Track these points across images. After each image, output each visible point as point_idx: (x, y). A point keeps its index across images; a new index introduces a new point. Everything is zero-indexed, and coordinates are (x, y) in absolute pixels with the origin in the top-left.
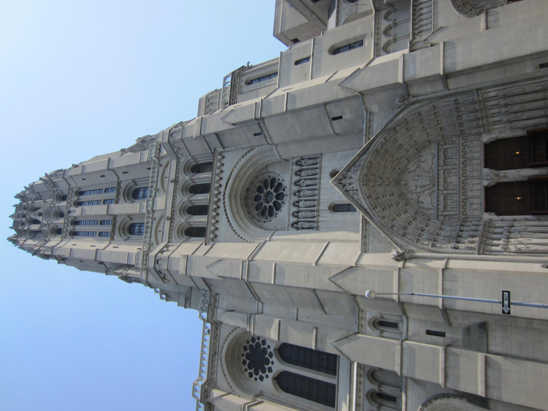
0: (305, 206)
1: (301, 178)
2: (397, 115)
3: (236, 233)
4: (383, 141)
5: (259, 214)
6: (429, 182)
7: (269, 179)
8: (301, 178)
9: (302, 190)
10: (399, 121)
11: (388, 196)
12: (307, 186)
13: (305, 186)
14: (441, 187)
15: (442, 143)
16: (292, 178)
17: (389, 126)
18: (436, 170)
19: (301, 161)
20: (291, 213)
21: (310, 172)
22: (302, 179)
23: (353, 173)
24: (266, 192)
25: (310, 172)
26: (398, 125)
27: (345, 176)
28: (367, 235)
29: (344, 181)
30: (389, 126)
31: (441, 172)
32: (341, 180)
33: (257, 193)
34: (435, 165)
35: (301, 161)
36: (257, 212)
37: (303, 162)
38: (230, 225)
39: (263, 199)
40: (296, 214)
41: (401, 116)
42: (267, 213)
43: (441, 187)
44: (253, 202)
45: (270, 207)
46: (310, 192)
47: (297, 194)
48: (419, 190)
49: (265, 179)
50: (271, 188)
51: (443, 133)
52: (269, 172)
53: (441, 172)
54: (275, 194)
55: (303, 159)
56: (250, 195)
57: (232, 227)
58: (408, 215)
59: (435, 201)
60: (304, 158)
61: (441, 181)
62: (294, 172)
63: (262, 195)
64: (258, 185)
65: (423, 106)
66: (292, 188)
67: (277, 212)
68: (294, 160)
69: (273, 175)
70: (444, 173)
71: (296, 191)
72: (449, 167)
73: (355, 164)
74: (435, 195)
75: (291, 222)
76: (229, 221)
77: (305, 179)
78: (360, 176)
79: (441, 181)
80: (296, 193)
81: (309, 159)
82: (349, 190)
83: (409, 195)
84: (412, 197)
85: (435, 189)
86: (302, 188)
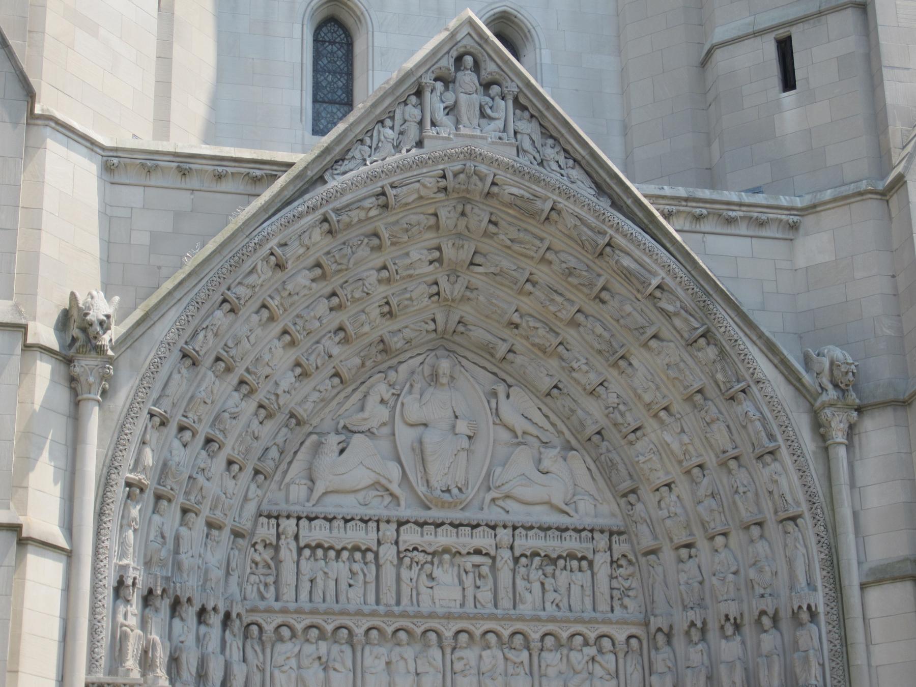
2: (771, 349)
4: (655, 282)
6: (438, 482)
10: (744, 357)
11: (381, 291)
14: (410, 536)
15: (620, 547)
17: (721, 311)
18: (494, 514)
23: (505, 129)
26: (722, 353)
27: (495, 89)
28: (194, 183)
29: (468, 79)
30: (721, 311)
31: (483, 540)
32: (477, 67)
34: (518, 514)
41: (765, 367)
43: (410, 536)
48: (405, 436)
51: (668, 555)
53: (483, 540)
58: (287, 380)
59: (349, 505)
61: (445, 538)
65: (802, 471)
70: (478, 552)
72: (505, 576)
73: (550, 142)
74: (378, 507)
78: (492, 162)
79: (445, 538)
82: (421, 105)
83: (382, 389)
84: (372, 402)
85: (406, 511)
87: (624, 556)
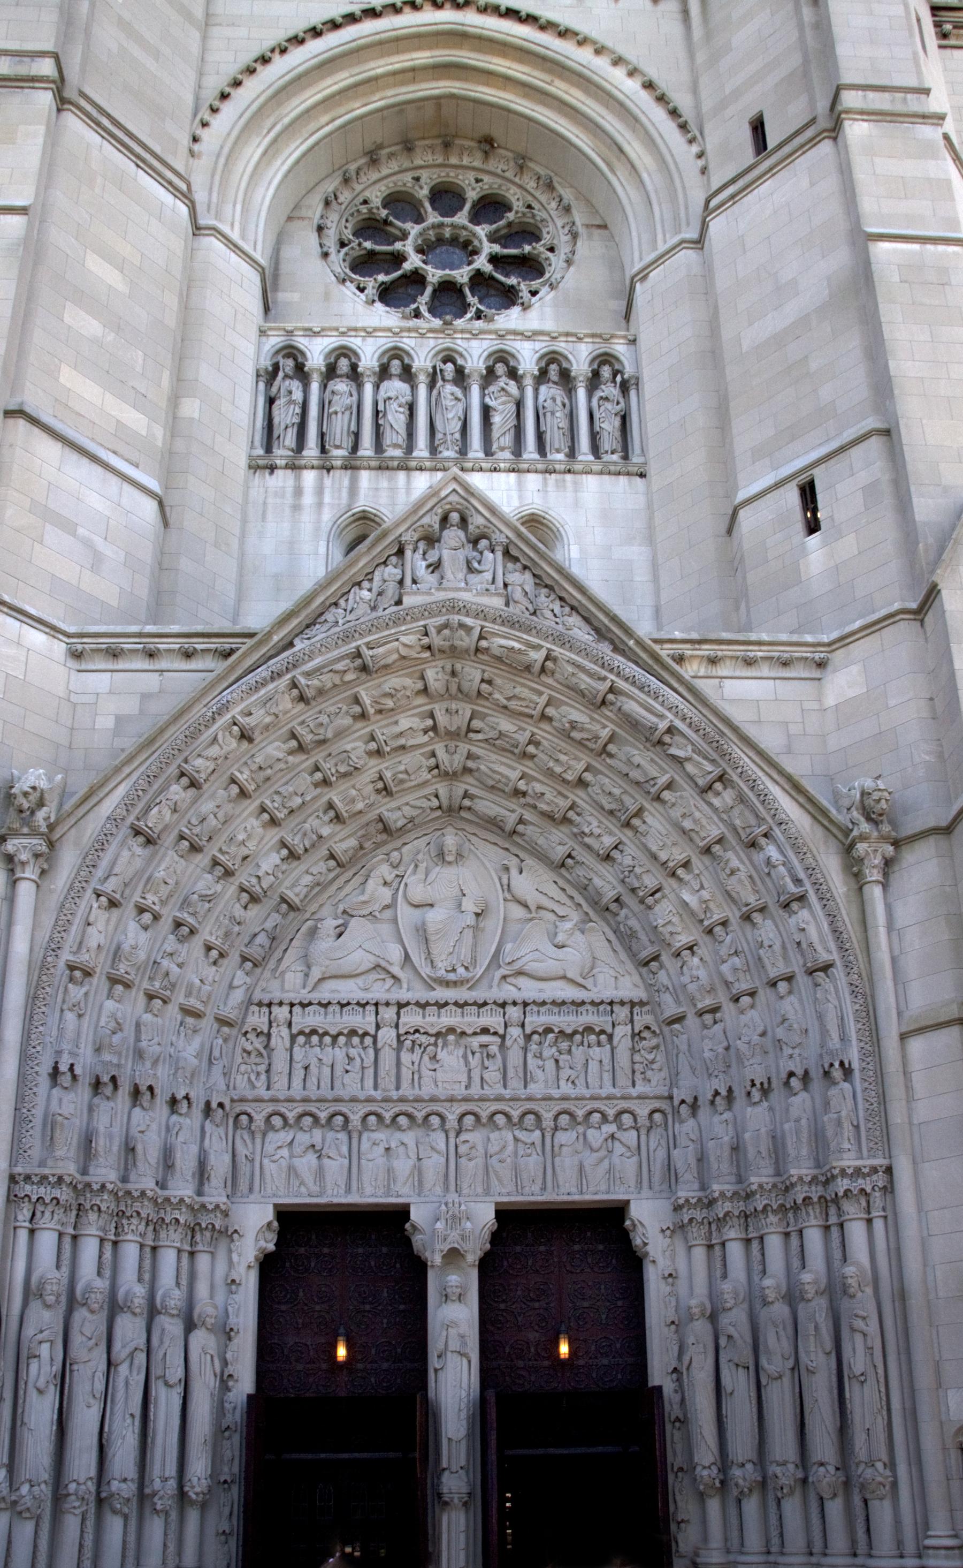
0: (381, 407)
1: (528, 382)
3: (251, 71)
5: (364, 209)
7: (540, 248)
8: (528, 382)
9: (466, 389)
12: (486, 412)
13: (487, 400)
16: (529, 338)
19: (614, 381)
20: (355, 342)
21: (555, 424)
22: (521, 388)
24: (474, 234)
25: (555, 424)
33: (472, 195)
35: (614, 381)
36: (376, 196)
37: (610, 390)
38: (297, 41)
39: (441, 225)
40: (344, 365)
42: (368, 245)
44: (429, 179)
45: (398, 259)
46: (456, 426)
47: (450, 367)
49: (544, 231)
50: (494, 259)
52: (575, 236)
54: (462, 275)
55: (625, 388)
56: (466, 161)
57: (283, 51)
60: (633, 393)
62: (561, 346)
63: (461, 218)
64: (514, 196)
66: (474, 343)
67: (371, 290)
68: (620, 348)
69: (556, 263)
71: (460, 362)
75: (302, 342)
76: (316, 32)
77: (519, 404)
80: (454, 362)
81: (624, 419)
86: (475, 390)
87: (648, 1028)
